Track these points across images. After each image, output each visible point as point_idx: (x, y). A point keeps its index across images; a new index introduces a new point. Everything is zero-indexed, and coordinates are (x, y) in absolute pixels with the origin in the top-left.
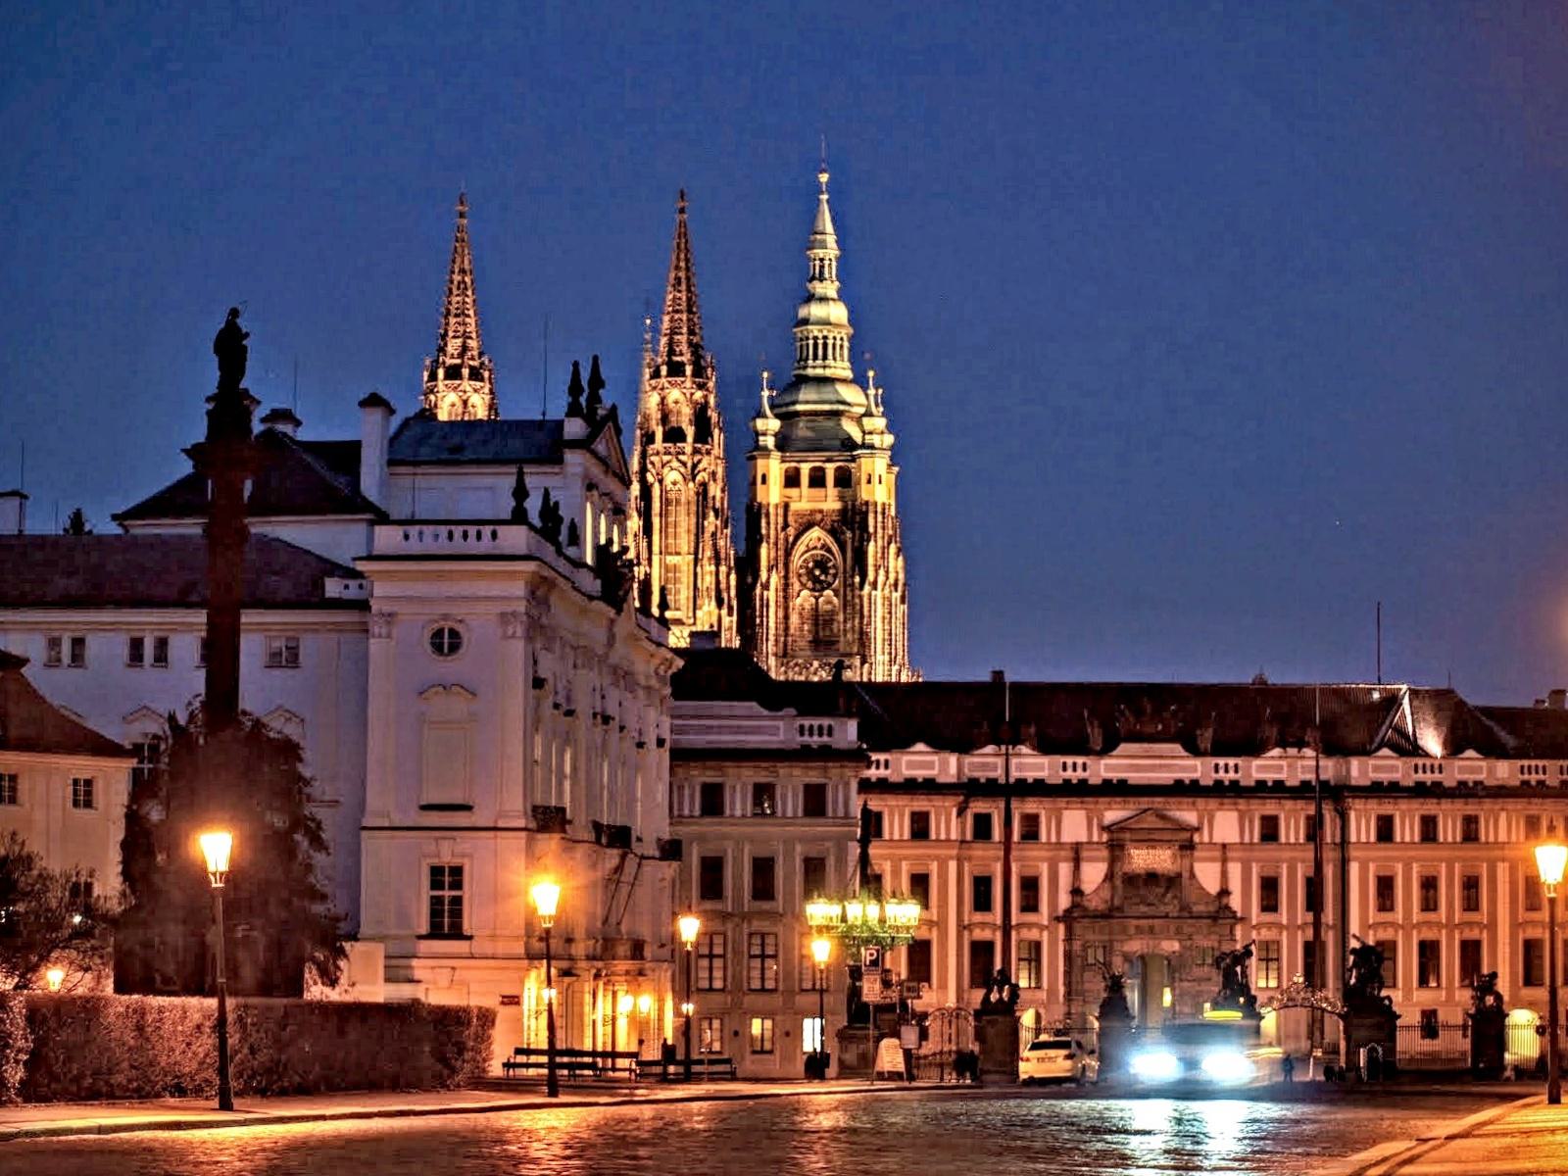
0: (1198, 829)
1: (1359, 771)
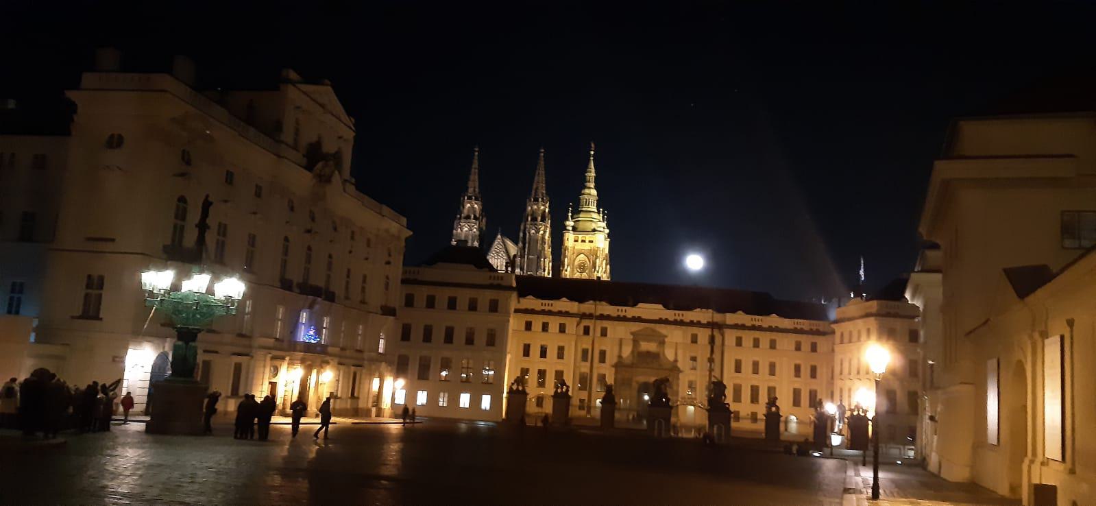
1: (730, 318)
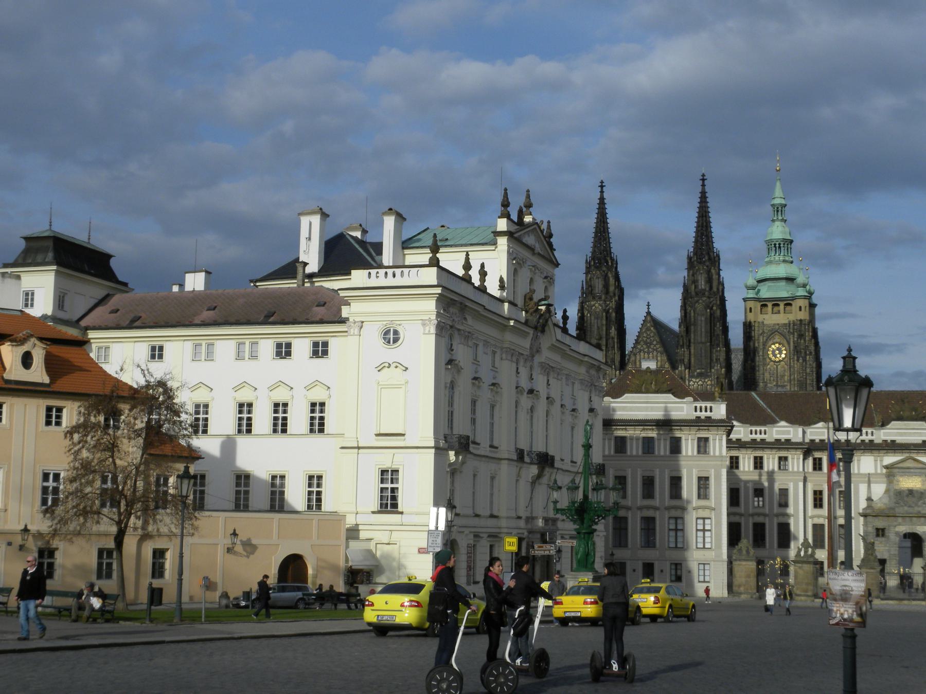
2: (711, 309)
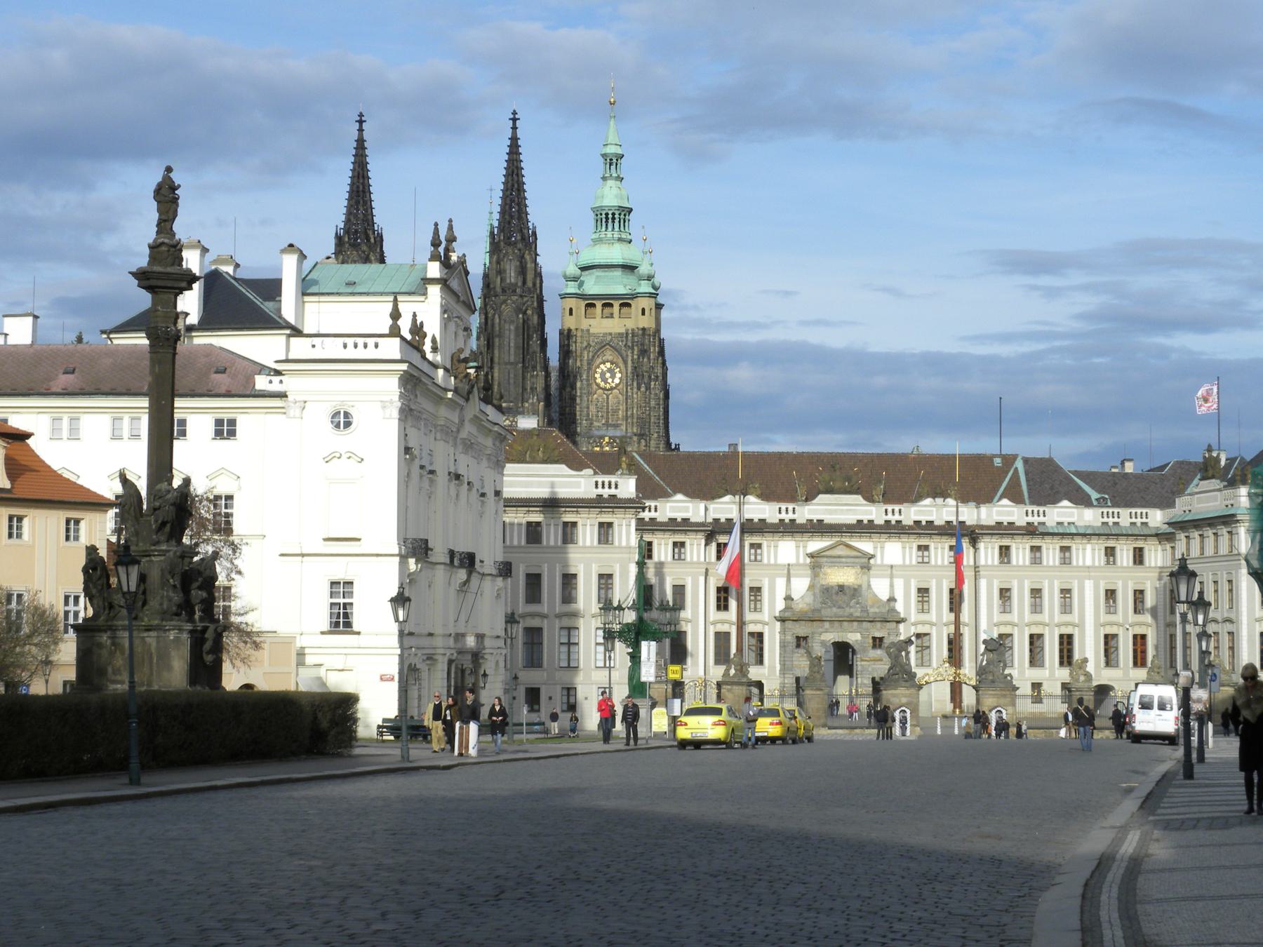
0: (872, 556)
2: (525, 313)
